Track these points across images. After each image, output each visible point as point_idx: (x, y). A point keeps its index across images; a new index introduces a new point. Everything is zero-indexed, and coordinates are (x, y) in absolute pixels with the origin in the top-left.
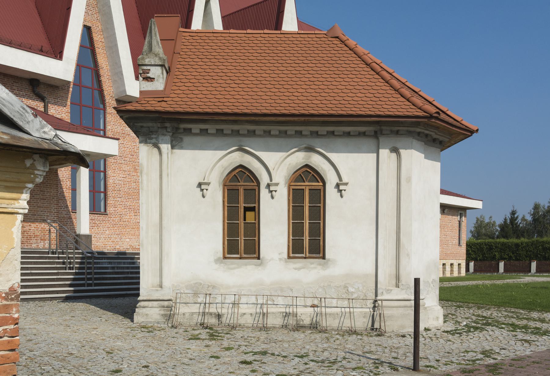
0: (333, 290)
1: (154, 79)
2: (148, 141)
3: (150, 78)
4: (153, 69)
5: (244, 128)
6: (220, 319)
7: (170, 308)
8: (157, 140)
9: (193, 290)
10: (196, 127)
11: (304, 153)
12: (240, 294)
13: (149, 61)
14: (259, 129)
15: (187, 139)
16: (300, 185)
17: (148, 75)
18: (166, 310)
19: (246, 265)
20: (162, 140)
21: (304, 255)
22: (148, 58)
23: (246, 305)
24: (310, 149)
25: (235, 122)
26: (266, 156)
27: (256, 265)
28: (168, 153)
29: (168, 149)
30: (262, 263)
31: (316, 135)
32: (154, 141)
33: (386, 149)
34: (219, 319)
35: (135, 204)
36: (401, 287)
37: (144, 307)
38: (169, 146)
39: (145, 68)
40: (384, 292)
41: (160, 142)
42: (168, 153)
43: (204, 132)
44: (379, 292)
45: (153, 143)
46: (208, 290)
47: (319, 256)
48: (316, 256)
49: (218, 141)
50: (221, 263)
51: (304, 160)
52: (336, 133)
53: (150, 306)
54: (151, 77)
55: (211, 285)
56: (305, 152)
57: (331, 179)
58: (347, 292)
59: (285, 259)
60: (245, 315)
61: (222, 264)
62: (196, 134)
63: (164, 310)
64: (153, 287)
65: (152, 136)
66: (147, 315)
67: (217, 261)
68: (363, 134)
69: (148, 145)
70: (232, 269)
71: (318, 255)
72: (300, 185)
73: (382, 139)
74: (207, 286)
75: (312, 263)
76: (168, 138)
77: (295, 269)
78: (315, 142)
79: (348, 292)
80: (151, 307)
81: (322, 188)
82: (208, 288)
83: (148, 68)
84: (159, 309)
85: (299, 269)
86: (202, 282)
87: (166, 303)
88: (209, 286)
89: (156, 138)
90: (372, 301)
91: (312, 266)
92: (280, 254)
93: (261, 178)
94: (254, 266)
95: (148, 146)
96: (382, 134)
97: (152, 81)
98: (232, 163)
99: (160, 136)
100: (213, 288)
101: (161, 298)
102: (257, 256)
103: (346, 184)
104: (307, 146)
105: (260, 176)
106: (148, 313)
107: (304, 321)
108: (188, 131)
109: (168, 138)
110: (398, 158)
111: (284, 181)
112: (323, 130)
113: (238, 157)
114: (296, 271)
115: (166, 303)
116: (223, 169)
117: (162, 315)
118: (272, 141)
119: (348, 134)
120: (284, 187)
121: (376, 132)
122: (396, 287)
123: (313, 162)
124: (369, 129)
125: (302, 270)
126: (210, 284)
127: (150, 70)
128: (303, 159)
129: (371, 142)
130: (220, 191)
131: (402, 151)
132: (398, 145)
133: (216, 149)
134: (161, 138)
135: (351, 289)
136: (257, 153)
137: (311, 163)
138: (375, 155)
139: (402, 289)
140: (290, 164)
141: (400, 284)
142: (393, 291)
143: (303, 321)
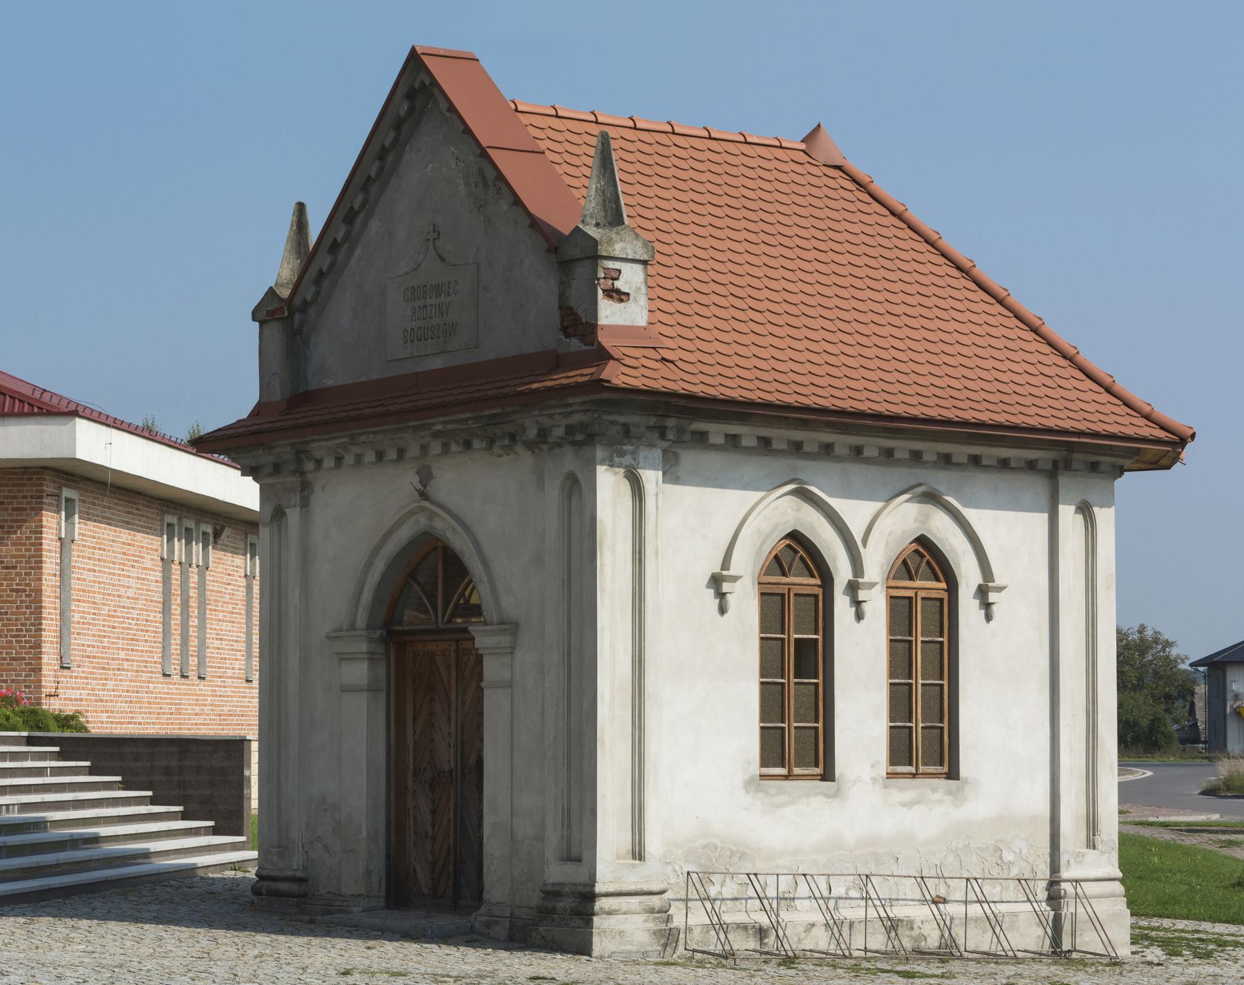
0: (974, 858)
1: (628, 294)
2: (617, 460)
3: (618, 292)
4: (626, 268)
5: (812, 438)
6: (766, 940)
7: (663, 913)
8: (635, 460)
9: (700, 865)
10: (717, 431)
11: (917, 505)
12: (795, 873)
13: (623, 249)
14: (842, 442)
15: (689, 458)
16: (908, 588)
17: (618, 284)
18: (659, 918)
19: (807, 795)
20: (646, 458)
21: (912, 769)
22: (621, 240)
23: (808, 901)
24: (932, 498)
25: (767, 421)
26: (856, 513)
27: (827, 796)
28: (657, 495)
29: (657, 484)
30: (839, 790)
31: (946, 461)
32: (627, 460)
33: (1070, 505)
34: (761, 939)
35: (17, 619)
36: (1100, 847)
37: (610, 913)
38: (660, 473)
39: (611, 264)
41: (640, 464)
42: (657, 495)
43: (733, 442)
44: (1064, 859)
45: (626, 467)
46: (731, 864)
47: (940, 771)
48: (935, 771)
49: (752, 467)
50: (758, 789)
51: (917, 525)
52: (984, 462)
53: (624, 909)
54: (623, 290)
55: (738, 851)
57: (968, 576)
58: (999, 862)
59: (883, 777)
60: (814, 929)
61: (760, 794)
62: (716, 447)
63: (655, 919)
64: (618, 857)
65: (625, 447)
66: (621, 933)
67: (748, 784)
68: (1031, 466)
69: (617, 470)
70: (778, 806)
71: (939, 769)
72: (908, 588)
73: (1064, 480)
74: (729, 854)
75: (934, 790)
76: (657, 454)
77: (903, 805)
78: (940, 480)
79: (1000, 863)
80: (625, 913)
81: (945, 595)
82: (731, 857)
83: (617, 265)
84: (644, 917)
85: (909, 805)
87: (655, 901)
88: (732, 854)
89: (633, 453)
90: (1044, 884)
91: (936, 796)
92: (873, 766)
93: (836, 568)
94: (822, 799)
95: (616, 474)
96: (1068, 466)
97: (622, 301)
98: (777, 525)
99: (641, 447)
101: (646, 887)
102: (822, 772)
103: (1000, 589)
104: (928, 490)
105: (834, 561)
106: (621, 927)
107: (928, 940)
108: (701, 439)
109: (657, 454)
110: (1086, 528)
111: (880, 576)
112: (961, 452)
113: (789, 510)
114: (905, 809)
115: (655, 901)
116: (761, 540)
117: (655, 933)
118: (857, 472)
119: (1004, 464)
120: (881, 592)
121: (1055, 463)
122: (1088, 846)
123: (935, 531)
124: (1042, 456)
125: (915, 808)
126: (734, 848)
127: (620, 271)
128: (916, 520)
129: (1036, 487)
130: (755, 597)
131: (1096, 510)
132: (1091, 498)
133: (747, 487)
134: (644, 452)
135: (1008, 856)
136: (835, 503)
137: (929, 531)
138: (1044, 517)
139: (1103, 853)
140: (890, 534)
141: (1098, 839)
142: (1086, 857)
143: (926, 940)
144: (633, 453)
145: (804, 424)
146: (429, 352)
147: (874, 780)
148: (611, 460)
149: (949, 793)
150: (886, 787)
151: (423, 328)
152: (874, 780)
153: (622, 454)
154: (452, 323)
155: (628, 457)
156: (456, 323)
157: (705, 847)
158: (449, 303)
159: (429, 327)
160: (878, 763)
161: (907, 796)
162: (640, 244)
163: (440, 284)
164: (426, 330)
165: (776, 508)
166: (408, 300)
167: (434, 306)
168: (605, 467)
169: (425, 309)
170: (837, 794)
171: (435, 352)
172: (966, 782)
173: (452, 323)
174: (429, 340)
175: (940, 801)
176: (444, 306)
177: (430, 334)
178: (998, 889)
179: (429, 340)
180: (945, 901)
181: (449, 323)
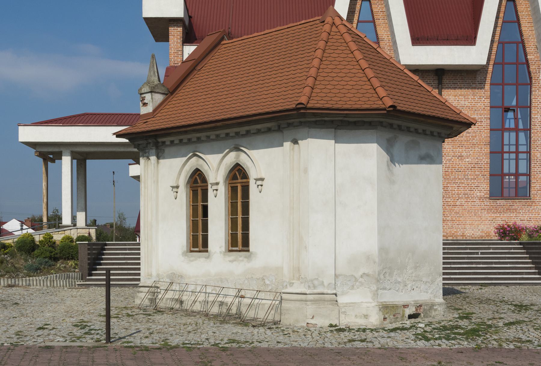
0: (255, 282)
1: (147, 103)
6: (182, 305)
15: (167, 150)
19: (200, 257)
24: (237, 149)
27: (206, 258)
30: (209, 256)
32: (147, 154)
33: (288, 142)
34: (181, 304)
40: (288, 285)
50: (186, 256)
56: (236, 151)
59: (224, 252)
61: (186, 257)
70: (192, 261)
74: (178, 276)
75: (241, 256)
76: (154, 151)
77: (230, 261)
82: (178, 277)
85: (231, 261)
86: (175, 273)
87: (152, 290)
88: (179, 276)
91: (241, 259)
92: (220, 247)
94: (204, 259)
98: (192, 167)
100: (181, 277)
105: (208, 176)
112: (243, 130)
114: (231, 263)
115: (152, 290)
123: (241, 161)
125: (234, 262)
126: (179, 275)
135: (267, 282)
140: (226, 164)
144: (148, 152)
145: (186, 132)
147: (221, 252)
148: (143, 155)
149: (246, 257)
150: (224, 255)
152: (221, 252)
153: (145, 153)
155: (147, 154)
157: (171, 273)
160: (222, 246)
161: (231, 258)
162: (148, 87)
165: (191, 162)
168: (142, 158)
170: (208, 257)
172: (252, 253)
175: (243, 261)
178: (264, 294)
180: (244, 297)
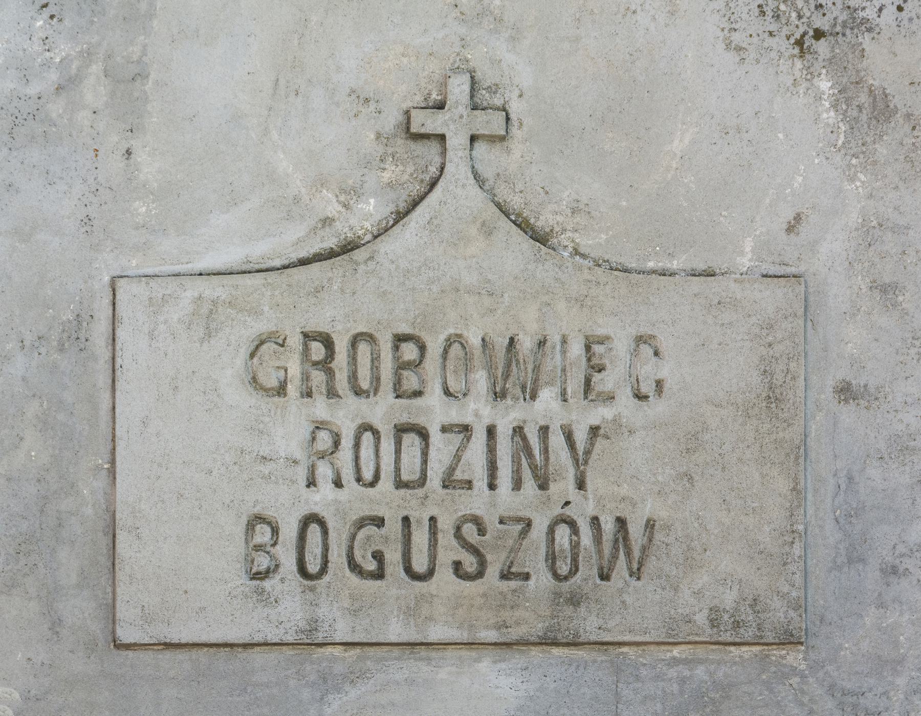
146: (436, 633)
151: (393, 527)
154: (621, 522)
156: (650, 525)
158: (594, 431)
159: (446, 524)
163: (526, 344)
164: (420, 538)
166: (281, 390)
167: (479, 440)
169: (411, 441)
171: (491, 635)
173: (621, 522)
174: (444, 576)
176: (557, 441)
177: (449, 551)
179: (444, 576)
181: (595, 521)
